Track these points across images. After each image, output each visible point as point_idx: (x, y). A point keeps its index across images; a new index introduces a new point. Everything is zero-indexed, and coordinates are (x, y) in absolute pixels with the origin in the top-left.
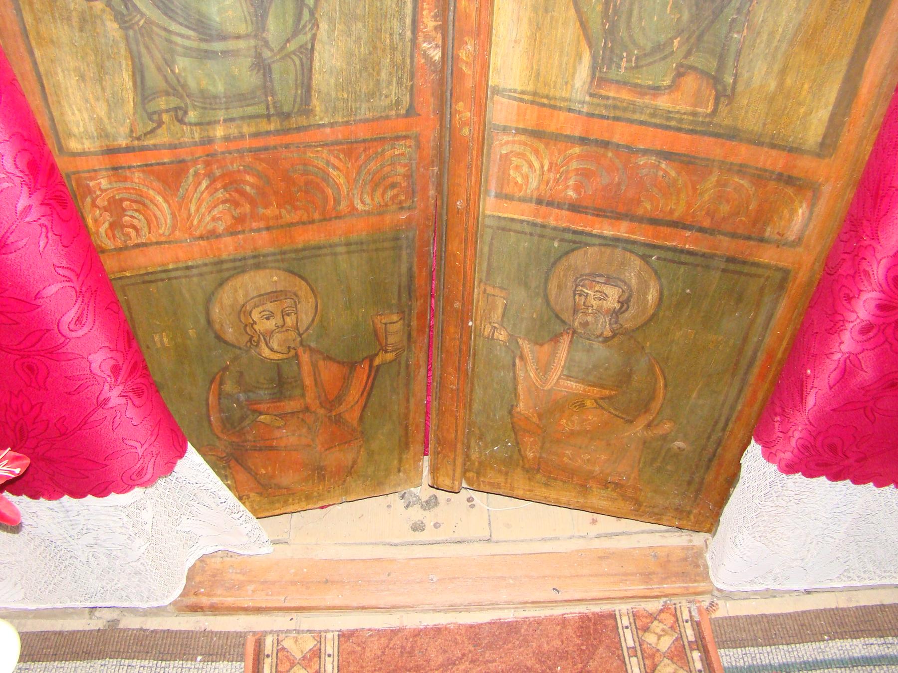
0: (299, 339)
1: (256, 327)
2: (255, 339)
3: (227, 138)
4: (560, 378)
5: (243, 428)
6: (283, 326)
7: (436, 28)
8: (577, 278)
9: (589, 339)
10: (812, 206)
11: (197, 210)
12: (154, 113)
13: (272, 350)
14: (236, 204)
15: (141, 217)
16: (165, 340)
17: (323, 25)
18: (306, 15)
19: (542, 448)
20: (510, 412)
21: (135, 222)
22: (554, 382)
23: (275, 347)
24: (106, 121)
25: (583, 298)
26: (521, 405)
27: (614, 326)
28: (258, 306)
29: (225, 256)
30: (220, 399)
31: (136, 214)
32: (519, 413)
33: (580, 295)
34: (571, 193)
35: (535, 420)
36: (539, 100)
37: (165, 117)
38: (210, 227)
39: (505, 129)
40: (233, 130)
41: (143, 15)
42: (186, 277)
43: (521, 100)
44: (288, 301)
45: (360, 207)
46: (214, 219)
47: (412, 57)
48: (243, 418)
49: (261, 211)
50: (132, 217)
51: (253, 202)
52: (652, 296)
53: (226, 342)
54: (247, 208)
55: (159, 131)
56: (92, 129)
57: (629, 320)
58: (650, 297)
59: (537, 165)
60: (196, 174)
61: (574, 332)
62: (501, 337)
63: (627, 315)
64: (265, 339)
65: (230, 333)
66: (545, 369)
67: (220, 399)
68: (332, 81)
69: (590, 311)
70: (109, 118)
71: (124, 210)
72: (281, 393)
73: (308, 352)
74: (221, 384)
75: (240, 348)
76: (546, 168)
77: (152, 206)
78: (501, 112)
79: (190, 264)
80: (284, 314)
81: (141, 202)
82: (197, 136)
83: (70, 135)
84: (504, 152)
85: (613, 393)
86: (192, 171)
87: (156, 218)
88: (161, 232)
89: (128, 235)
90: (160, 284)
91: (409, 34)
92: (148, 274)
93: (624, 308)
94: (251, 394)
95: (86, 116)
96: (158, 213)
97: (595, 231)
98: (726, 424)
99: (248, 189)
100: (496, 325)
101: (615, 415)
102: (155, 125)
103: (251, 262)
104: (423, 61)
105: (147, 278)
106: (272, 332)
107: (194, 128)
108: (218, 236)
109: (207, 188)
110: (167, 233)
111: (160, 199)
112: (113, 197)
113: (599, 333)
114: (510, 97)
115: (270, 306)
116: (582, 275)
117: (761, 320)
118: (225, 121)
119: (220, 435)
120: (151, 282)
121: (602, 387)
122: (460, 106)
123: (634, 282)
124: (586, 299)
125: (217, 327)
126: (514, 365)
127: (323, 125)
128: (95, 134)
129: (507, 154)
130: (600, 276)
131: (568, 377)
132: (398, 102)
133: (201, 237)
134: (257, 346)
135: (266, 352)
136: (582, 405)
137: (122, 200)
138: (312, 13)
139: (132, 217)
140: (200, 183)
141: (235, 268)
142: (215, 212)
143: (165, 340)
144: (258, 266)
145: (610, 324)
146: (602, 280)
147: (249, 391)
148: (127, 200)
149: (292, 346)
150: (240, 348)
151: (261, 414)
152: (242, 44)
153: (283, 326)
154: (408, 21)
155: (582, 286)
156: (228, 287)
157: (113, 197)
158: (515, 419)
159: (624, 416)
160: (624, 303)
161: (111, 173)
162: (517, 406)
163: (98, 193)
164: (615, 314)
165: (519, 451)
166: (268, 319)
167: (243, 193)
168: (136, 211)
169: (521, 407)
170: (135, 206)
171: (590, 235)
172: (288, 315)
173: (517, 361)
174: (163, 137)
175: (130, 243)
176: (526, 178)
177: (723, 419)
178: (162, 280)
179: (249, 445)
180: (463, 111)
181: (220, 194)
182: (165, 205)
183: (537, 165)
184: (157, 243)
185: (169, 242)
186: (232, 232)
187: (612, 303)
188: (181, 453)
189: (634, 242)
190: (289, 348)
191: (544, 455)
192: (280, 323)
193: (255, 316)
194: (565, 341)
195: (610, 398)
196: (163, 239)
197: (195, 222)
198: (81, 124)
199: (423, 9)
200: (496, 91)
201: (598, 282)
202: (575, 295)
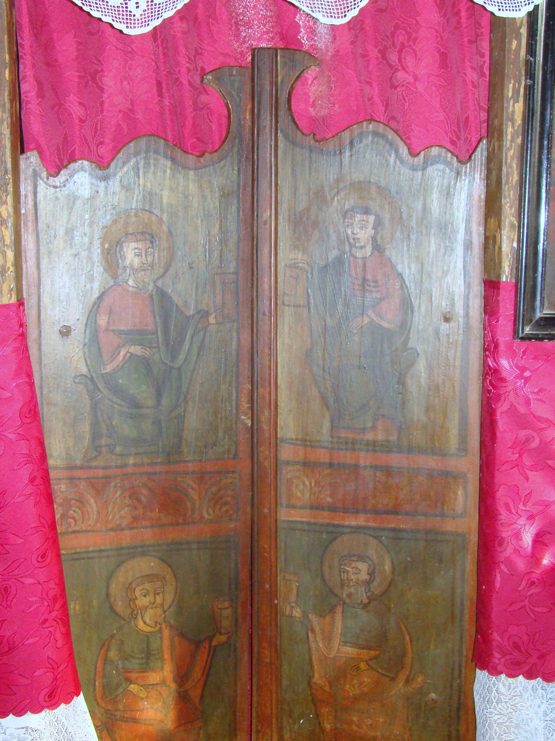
0: (163, 615)
1: (137, 602)
2: (135, 612)
3: (135, 465)
4: (339, 645)
5: (116, 696)
6: (154, 603)
7: (248, 407)
8: (340, 559)
9: (354, 608)
10: (465, 488)
11: (113, 510)
12: (98, 447)
13: (145, 623)
14: (135, 508)
15: (80, 512)
16: (77, 607)
17: (190, 404)
18: (182, 398)
19: (335, 717)
20: (309, 684)
21: (76, 515)
22: (336, 650)
23: (148, 621)
24: (72, 449)
25: (346, 574)
26: (316, 675)
27: (368, 594)
28: (139, 585)
29: (124, 544)
30: (105, 664)
31: (77, 510)
32: (315, 683)
33: (344, 572)
34: (329, 499)
35: (327, 688)
36: (306, 442)
37: (104, 449)
38: (118, 522)
39: (288, 463)
40: (138, 460)
41: (101, 392)
42: (99, 557)
43: (297, 445)
44: (159, 582)
45: (206, 516)
46: (121, 517)
47: (236, 423)
48: (118, 686)
49: (149, 514)
50: (74, 511)
51: (145, 508)
52: (387, 567)
53: (116, 613)
54: (140, 511)
55: (99, 458)
56: (64, 454)
57: (377, 587)
58: (386, 567)
59: (307, 483)
60: (115, 486)
61: (344, 603)
62: (298, 615)
63: (375, 584)
64: (141, 613)
65: (120, 606)
66: (328, 638)
67: (105, 664)
68: (194, 435)
69: (352, 584)
70: (74, 447)
71: (71, 506)
72: (147, 663)
73: (168, 628)
74: (108, 650)
75: (124, 619)
76: (313, 485)
77: (87, 505)
78: (286, 453)
79: (103, 548)
80: (156, 594)
81: (81, 502)
82: (119, 462)
83: (51, 456)
84: (289, 477)
85: (377, 652)
86: (113, 484)
87: (88, 512)
88: (89, 523)
89: (70, 524)
90: (82, 561)
91: (234, 411)
92: (76, 553)
93: (372, 579)
94: (126, 662)
95: (62, 445)
96: (90, 510)
97: (346, 523)
98: (460, 671)
99: (143, 498)
100: (293, 604)
101: (383, 674)
102: (97, 454)
103: (139, 550)
104: (242, 426)
105: (75, 556)
106: (146, 608)
107: (118, 457)
108: (122, 529)
109: (120, 495)
110: (92, 525)
111: (92, 501)
112: (66, 497)
113: (359, 601)
114: (290, 443)
115: (147, 586)
116: (342, 557)
117: (458, 575)
118: (135, 454)
119: (100, 701)
120: (77, 559)
121: (369, 648)
122: (262, 449)
123: (375, 557)
124: (348, 574)
125: (112, 599)
126: (308, 638)
127: (188, 461)
128: (65, 457)
129: (290, 479)
130: (354, 555)
131: (345, 643)
132: (229, 450)
133: (112, 530)
134: (136, 618)
135: (141, 625)
136: (358, 668)
137: (70, 500)
138: (185, 397)
139: (74, 511)
140: (116, 492)
141: (129, 554)
142: (122, 512)
143: (77, 607)
144: (144, 554)
145: (366, 593)
146: (355, 558)
147: (126, 659)
148: (74, 500)
149: (159, 621)
150: (124, 619)
151: (131, 683)
152: (148, 411)
153: (154, 603)
154: (234, 403)
155: (344, 565)
156: (122, 569)
157: (66, 497)
158: (313, 690)
159: (389, 674)
160: (371, 574)
161: (68, 481)
162: (313, 677)
163: (59, 494)
164: (368, 583)
165: (319, 723)
166: (145, 596)
167: (139, 500)
168: (78, 507)
169: (317, 678)
170: (77, 504)
171: (343, 526)
172: (158, 594)
173: (310, 634)
174: (100, 462)
175: (70, 530)
176: (302, 492)
177: (457, 667)
178: (83, 559)
179: (118, 714)
180: (264, 451)
181: (127, 501)
182: (94, 505)
183: (307, 483)
184: (86, 531)
185: (93, 531)
186: (130, 527)
187: (364, 576)
188: (78, 695)
189: (369, 528)
190: (156, 622)
191: (338, 726)
192: (152, 601)
193: (138, 593)
194: (339, 609)
195: (376, 658)
196: (90, 528)
197: (110, 518)
198: (59, 450)
199: (241, 397)
200: (283, 440)
201: (353, 561)
202: (340, 572)
